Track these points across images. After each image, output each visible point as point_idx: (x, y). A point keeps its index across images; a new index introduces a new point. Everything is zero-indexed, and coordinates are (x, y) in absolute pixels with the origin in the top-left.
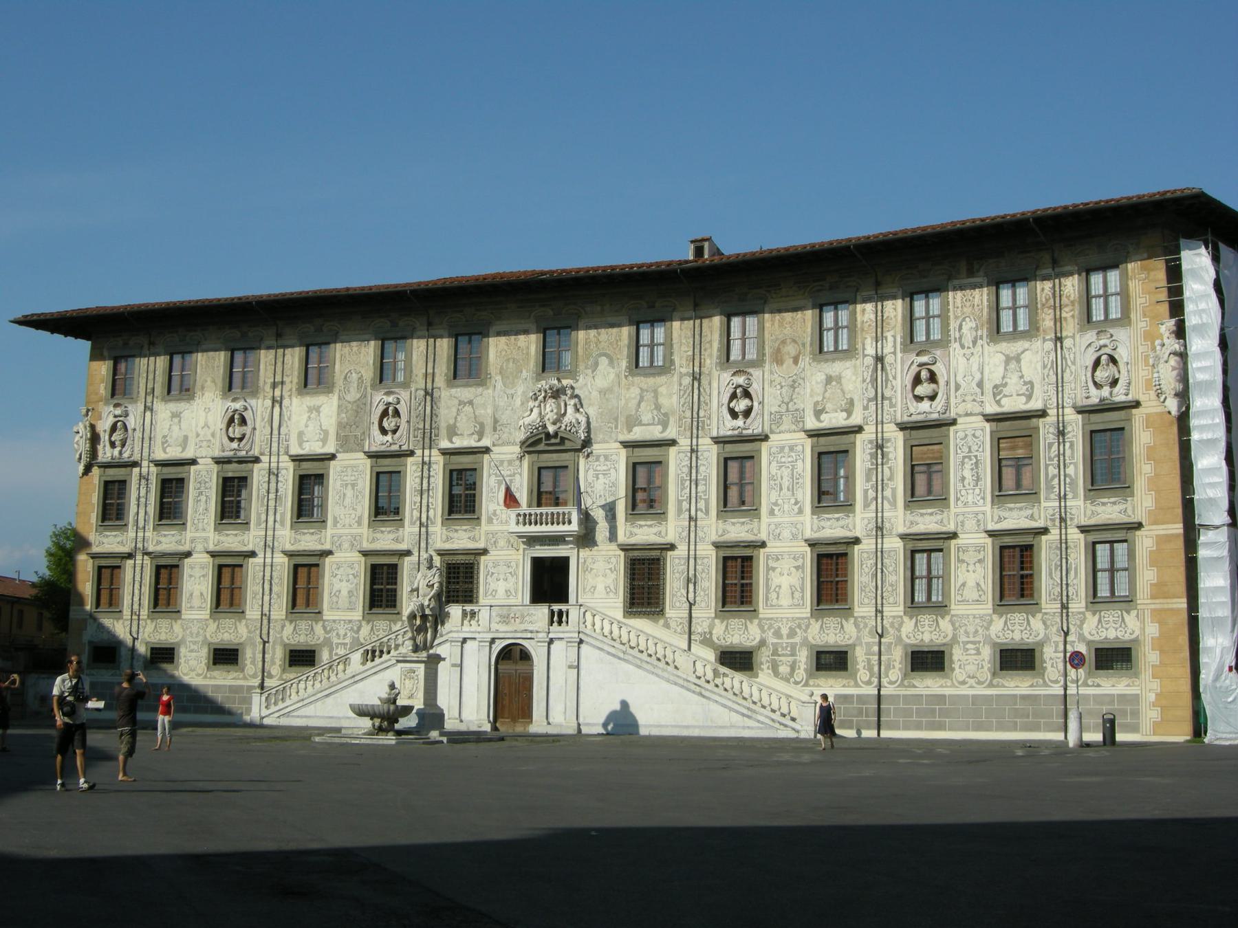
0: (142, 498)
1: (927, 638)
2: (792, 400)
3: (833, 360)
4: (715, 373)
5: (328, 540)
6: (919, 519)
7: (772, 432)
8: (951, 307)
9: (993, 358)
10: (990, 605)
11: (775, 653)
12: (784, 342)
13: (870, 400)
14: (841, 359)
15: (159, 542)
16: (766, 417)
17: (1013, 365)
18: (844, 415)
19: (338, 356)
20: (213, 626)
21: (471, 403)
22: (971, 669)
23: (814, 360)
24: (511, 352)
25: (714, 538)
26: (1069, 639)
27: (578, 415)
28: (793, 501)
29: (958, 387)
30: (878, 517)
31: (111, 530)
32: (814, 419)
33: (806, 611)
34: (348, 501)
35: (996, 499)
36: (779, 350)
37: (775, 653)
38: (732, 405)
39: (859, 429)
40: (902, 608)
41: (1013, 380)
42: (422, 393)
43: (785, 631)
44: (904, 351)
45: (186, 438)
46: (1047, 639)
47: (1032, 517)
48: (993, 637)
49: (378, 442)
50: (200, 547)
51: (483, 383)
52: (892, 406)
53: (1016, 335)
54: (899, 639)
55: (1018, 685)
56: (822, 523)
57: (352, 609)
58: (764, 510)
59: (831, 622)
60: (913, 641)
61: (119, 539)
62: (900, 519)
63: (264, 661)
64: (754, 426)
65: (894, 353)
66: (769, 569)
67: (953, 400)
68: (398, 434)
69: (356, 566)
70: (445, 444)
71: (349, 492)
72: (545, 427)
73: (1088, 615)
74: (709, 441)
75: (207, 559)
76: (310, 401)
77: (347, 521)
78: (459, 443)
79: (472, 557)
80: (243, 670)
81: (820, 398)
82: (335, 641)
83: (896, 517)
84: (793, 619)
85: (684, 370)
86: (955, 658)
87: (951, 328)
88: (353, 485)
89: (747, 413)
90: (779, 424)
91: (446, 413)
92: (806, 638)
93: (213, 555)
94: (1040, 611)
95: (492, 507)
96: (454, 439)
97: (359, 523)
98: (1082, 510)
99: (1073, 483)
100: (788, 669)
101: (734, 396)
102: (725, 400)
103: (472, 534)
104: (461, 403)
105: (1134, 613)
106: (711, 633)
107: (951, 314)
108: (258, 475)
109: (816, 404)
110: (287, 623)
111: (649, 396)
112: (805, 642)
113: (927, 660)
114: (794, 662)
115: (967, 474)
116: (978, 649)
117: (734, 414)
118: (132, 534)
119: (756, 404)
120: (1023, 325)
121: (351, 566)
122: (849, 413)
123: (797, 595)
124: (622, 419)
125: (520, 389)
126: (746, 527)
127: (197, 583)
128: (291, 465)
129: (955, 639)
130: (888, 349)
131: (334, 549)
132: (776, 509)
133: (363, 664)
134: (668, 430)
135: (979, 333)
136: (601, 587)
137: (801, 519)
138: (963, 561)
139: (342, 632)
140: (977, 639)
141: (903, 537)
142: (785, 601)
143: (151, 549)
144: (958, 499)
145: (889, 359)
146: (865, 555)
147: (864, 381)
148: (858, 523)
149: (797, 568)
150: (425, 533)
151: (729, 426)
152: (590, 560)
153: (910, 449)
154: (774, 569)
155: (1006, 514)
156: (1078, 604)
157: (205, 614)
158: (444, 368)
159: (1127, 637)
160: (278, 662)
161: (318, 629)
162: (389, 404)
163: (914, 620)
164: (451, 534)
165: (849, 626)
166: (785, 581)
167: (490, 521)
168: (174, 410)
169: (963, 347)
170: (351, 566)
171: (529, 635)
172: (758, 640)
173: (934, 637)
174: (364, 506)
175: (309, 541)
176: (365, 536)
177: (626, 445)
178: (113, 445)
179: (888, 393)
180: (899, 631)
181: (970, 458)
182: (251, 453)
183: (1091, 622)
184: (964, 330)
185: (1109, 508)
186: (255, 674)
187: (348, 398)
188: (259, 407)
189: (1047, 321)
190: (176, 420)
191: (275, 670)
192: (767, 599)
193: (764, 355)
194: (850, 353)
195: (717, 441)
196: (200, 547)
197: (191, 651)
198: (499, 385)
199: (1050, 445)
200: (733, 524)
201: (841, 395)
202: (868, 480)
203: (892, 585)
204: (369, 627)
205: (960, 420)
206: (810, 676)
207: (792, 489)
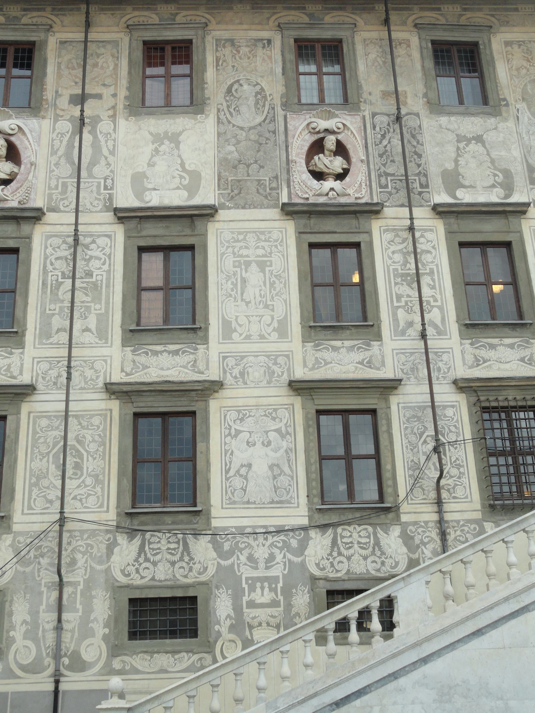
19: (210, 59)
21: (479, 139)
34: (251, 292)
51: (496, 113)
63: (59, 627)
69: (284, 414)
70: (442, 198)
71: (254, 276)
77: (255, 329)
82: (246, 572)
88: (262, 266)
97: (282, 331)
103: (527, 353)
104: (460, 138)
110: (122, 539)
121: (272, 414)
139: (261, 554)
158: (420, 87)
160: (100, 630)
161: (202, 549)
164: (483, 353)
170: (272, 414)
175: (165, 365)
176: (298, 357)
186: (38, 660)
187: (238, 121)
191: (94, 650)
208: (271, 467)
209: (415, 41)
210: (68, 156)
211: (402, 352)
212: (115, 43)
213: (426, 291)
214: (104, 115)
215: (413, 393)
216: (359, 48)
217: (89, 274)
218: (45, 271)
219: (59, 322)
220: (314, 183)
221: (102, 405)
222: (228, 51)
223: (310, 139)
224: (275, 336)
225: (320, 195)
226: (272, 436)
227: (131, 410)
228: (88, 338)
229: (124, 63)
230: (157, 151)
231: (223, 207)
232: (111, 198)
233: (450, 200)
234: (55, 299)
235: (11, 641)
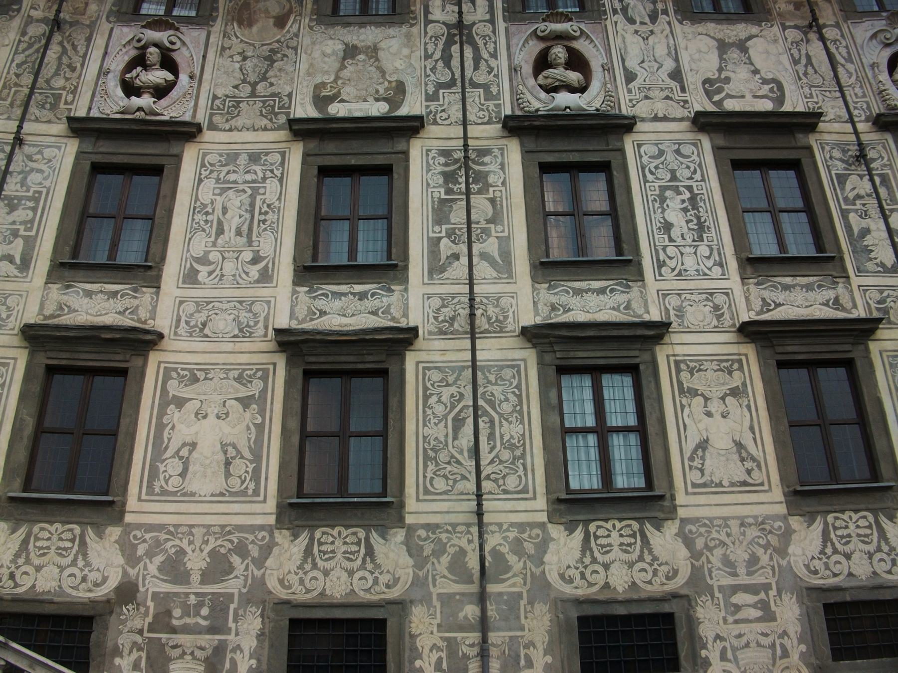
1: (619, 579)
2: (264, 78)
3: (362, 25)
4: (105, 26)
7: (213, 127)
10: (777, 494)
13: (440, 86)
14: (378, 24)
16: (202, 102)
23: (319, 22)
28: (248, 256)
29: (630, 77)
33: (264, 510)
35: (749, 270)
37: (162, 622)
40: (541, 503)
43: (196, 562)
48: (802, 572)
54: (540, 585)
56: (321, 303)
60: (581, 591)
62: (526, 301)
65: (492, 21)
66: (166, 401)
83: (514, 295)
84: (224, 531)
85: (37, 14)
86: (706, 631)
89: (161, 92)
101: (139, 61)
102: (117, 63)
109: (318, 87)
112: (257, 594)
114: (220, 650)
115: (674, 216)
116: (764, 605)
117: (130, 89)
119: (183, 78)
132: (203, 270)
137: (264, 292)
138: (694, 393)
140: (758, 579)
142: (205, 480)
144: (661, 265)
145: (482, 29)
146: (436, 376)
147: (427, 57)
149: (245, 402)
154: (180, 403)
155: (781, 297)
163: (579, 534)
165: (392, 551)
169: (632, 21)
173: (640, 578)
179: (481, 77)
192: (154, 474)
199: (842, 179)
200: (89, 294)
201: (376, 75)
203: (512, 447)
207: (247, 234)
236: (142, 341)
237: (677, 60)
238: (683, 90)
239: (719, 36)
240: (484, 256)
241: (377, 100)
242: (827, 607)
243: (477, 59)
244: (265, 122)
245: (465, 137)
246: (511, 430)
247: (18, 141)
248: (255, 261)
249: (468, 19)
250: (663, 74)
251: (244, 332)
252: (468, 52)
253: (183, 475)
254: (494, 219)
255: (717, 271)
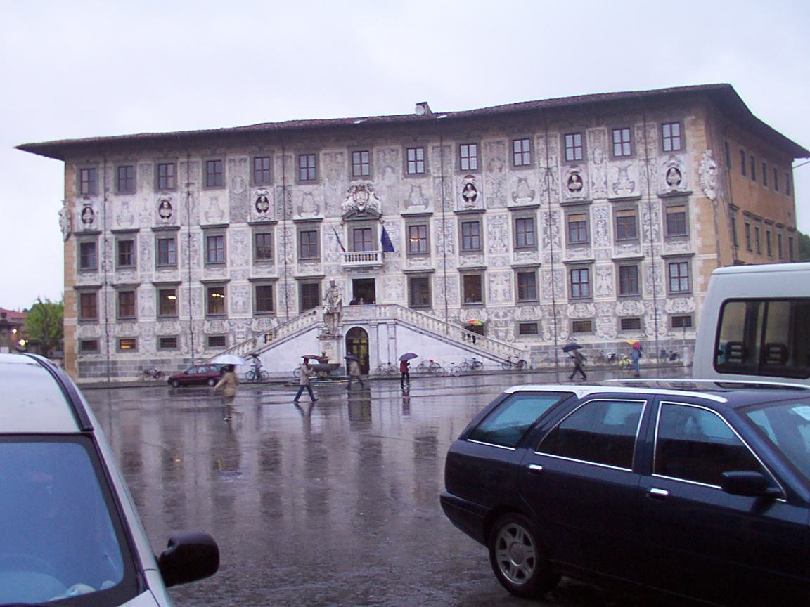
0: (107, 252)
1: (581, 315)
5: (229, 273)
6: (574, 253)
7: (489, 208)
8: (588, 142)
9: (612, 170)
10: (615, 297)
11: (496, 326)
12: (493, 160)
15: (119, 279)
16: (485, 199)
17: (623, 173)
18: (530, 199)
19: (227, 168)
20: (158, 326)
21: (311, 194)
22: (606, 330)
24: (332, 163)
25: (459, 266)
26: (657, 313)
27: (376, 200)
28: (502, 245)
29: (593, 184)
30: (552, 253)
31: (88, 273)
32: (512, 201)
33: (513, 303)
34: (239, 251)
35: (616, 243)
36: (490, 164)
37: (496, 326)
38: (464, 194)
39: (537, 207)
40: (567, 300)
41: (623, 180)
42: (281, 188)
43: (501, 314)
44: (563, 165)
45: (133, 216)
46: (646, 313)
47: (636, 252)
49: (255, 216)
50: (147, 280)
52: (557, 194)
53: (623, 157)
54: (566, 317)
55: (632, 338)
57: (245, 312)
58: (486, 250)
59: (527, 308)
61: (93, 278)
62: (564, 254)
63: (192, 344)
64: (478, 205)
65: (557, 166)
66: (491, 281)
67: (591, 192)
68: (268, 212)
70: (296, 217)
71: (240, 246)
72: (356, 207)
73: (668, 300)
74: (452, 213)
75: (150, 287)
76: (210, 193)
78: (304, 216)
79: (317, 281)
80: (179, 350)
81: (515, 190)
82: (237, 330)
84: (505, 308)
85: (436, 175)
86: (597, 325)
87: (588, 153)
88: (242, 242)
89: (474, 198)
90: (492, 204)
91: (296, 202)
92: (513, 318)
93: (155, 284)
94: (642, 299)
95: (327, 252)
96: (302, 215)
97: (247, 263)
98: (663, 248)
99: (658, 233)
100: (504, 334)
101: (466, 189)
102: (462, 191)
103: (316, 268)
104: (306, 194)
105: (692, 298)
106: (459, 317)
107: (588, 146)
108: (181, 238)
110: (206, 322)
111: (416, 189)
113: (581, 326)
115: (600, 229)
116: (609, 320)
117: (466, 199)
118: (101, 274)
119: (478, 193)
120: (627, 152)
122: (533, 198)
123: (507, 295)
124: (401, 203)
125: (340, 186)
126: (476, 260)
127: (147, 302)
128: (202, 232)
129: (596, 315)
130: (552, 164)
131: (232, 278)
132: (493, 249)
133: (266, 342)
134: (429, 208)
135: (604, 156)
136: (394, 295)
137: (507, 254)
138: (599, 275)
139: (240, 325)
141: (566, 263)
142: (501, 298)
143: (115, 283)
145: (554, 169)
147: (540, 181)
148: (540, 256)
149: (506, 281)
150: (287, 266)
151: (463, 205)
152: (386, 280)
153: (568, 216)
154: (493, 281)
156: (662, 295)
157: (154, 319)
159: (689, 311)
160: (202, 344)
161: (226, 324)
162: (262, 195)
164: (304, 268)
165: (537, 310)
166: (500, 289)
167: (326, 260)
168: (124, 200)
169: (595, 163)
171: (365, 322)
172: (486, 320)
174: (250, 254)
175: (216, 275)
177: (404, 216)
178: (84, 222)
179: (554, 188)
180: (565, 311)
181: (601, 221)
182: (175, 225)
183: (670, 303)
184: (596, 154)
185: (677, 246)
188: (177, 198)
189: (640, 149)
190: (125, 206)
191: (201, 349)
192: (490, 297)
193: (482, 167)
194: (530, 166)
195: (457, 213)
196: (147, 280)
197: (146, 341)
198: (327, 183)
199: (645, 214)
200: (469, 258)
201: (527, 188)
202: (545, 232)
203: (560, 288)
204: (257, 322)
205: (595, 201)
206: (517, 337)
207: (501, 239)
208: (244, 303)
209: (293, 156)
210: (186, 206)
211: (279, 268)
212: (197, 162)
213: (288, 249)
214: (196, 190)
215: (282, 281)
216: (275, 160)
217: (194, 246)
218: (182, 246)
219: (187, 262)
220: (258, 214)
221: (200, 286)
222: (232, 164)
223: (258, 197)
224: (245, 265)
225: (259, 218)
226: (244, 294)
227: (207, 287)
228: (195, 266)
229: (201, 170)
230: (211, 204)
231: (231, 223)
232: (199, 220)
233: (299, 218)
234: (185, 255)
235: (181, 347)
236: (484, 269)
237: (606, 178)
238: (607, 188)
239: (620, 166)
240: (556, 243)
241: (529, 197)
242: (622, 320)
243: (553, 180)
244: (501, 206)
245: (550, 208)
246: (560, 285)
247: (444, 219)
248: (504, 246)
249: (550, 167)
250: (602, 183)
251: (504, 264)
252: (550, 177)
253: (496, 297)
254: (557, 233)
255: (608, 244)
